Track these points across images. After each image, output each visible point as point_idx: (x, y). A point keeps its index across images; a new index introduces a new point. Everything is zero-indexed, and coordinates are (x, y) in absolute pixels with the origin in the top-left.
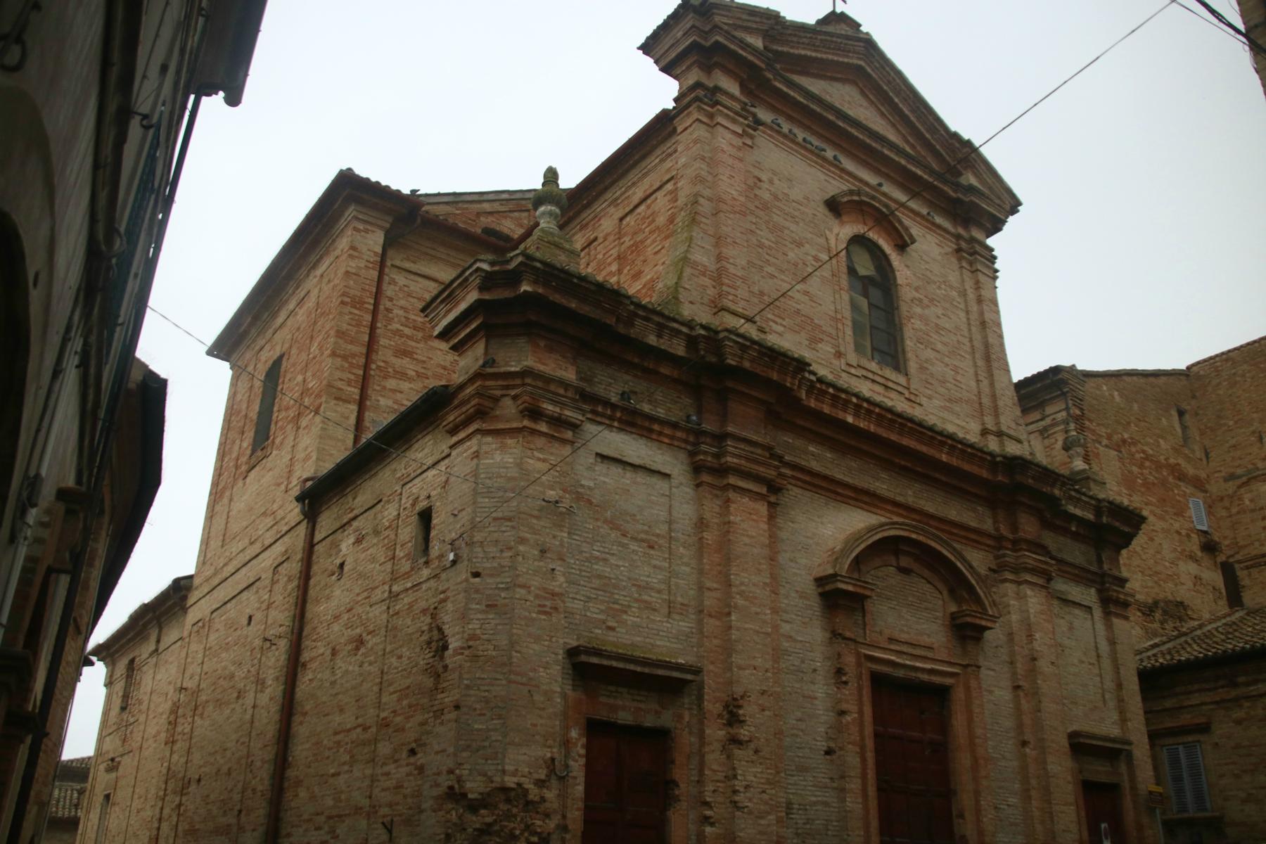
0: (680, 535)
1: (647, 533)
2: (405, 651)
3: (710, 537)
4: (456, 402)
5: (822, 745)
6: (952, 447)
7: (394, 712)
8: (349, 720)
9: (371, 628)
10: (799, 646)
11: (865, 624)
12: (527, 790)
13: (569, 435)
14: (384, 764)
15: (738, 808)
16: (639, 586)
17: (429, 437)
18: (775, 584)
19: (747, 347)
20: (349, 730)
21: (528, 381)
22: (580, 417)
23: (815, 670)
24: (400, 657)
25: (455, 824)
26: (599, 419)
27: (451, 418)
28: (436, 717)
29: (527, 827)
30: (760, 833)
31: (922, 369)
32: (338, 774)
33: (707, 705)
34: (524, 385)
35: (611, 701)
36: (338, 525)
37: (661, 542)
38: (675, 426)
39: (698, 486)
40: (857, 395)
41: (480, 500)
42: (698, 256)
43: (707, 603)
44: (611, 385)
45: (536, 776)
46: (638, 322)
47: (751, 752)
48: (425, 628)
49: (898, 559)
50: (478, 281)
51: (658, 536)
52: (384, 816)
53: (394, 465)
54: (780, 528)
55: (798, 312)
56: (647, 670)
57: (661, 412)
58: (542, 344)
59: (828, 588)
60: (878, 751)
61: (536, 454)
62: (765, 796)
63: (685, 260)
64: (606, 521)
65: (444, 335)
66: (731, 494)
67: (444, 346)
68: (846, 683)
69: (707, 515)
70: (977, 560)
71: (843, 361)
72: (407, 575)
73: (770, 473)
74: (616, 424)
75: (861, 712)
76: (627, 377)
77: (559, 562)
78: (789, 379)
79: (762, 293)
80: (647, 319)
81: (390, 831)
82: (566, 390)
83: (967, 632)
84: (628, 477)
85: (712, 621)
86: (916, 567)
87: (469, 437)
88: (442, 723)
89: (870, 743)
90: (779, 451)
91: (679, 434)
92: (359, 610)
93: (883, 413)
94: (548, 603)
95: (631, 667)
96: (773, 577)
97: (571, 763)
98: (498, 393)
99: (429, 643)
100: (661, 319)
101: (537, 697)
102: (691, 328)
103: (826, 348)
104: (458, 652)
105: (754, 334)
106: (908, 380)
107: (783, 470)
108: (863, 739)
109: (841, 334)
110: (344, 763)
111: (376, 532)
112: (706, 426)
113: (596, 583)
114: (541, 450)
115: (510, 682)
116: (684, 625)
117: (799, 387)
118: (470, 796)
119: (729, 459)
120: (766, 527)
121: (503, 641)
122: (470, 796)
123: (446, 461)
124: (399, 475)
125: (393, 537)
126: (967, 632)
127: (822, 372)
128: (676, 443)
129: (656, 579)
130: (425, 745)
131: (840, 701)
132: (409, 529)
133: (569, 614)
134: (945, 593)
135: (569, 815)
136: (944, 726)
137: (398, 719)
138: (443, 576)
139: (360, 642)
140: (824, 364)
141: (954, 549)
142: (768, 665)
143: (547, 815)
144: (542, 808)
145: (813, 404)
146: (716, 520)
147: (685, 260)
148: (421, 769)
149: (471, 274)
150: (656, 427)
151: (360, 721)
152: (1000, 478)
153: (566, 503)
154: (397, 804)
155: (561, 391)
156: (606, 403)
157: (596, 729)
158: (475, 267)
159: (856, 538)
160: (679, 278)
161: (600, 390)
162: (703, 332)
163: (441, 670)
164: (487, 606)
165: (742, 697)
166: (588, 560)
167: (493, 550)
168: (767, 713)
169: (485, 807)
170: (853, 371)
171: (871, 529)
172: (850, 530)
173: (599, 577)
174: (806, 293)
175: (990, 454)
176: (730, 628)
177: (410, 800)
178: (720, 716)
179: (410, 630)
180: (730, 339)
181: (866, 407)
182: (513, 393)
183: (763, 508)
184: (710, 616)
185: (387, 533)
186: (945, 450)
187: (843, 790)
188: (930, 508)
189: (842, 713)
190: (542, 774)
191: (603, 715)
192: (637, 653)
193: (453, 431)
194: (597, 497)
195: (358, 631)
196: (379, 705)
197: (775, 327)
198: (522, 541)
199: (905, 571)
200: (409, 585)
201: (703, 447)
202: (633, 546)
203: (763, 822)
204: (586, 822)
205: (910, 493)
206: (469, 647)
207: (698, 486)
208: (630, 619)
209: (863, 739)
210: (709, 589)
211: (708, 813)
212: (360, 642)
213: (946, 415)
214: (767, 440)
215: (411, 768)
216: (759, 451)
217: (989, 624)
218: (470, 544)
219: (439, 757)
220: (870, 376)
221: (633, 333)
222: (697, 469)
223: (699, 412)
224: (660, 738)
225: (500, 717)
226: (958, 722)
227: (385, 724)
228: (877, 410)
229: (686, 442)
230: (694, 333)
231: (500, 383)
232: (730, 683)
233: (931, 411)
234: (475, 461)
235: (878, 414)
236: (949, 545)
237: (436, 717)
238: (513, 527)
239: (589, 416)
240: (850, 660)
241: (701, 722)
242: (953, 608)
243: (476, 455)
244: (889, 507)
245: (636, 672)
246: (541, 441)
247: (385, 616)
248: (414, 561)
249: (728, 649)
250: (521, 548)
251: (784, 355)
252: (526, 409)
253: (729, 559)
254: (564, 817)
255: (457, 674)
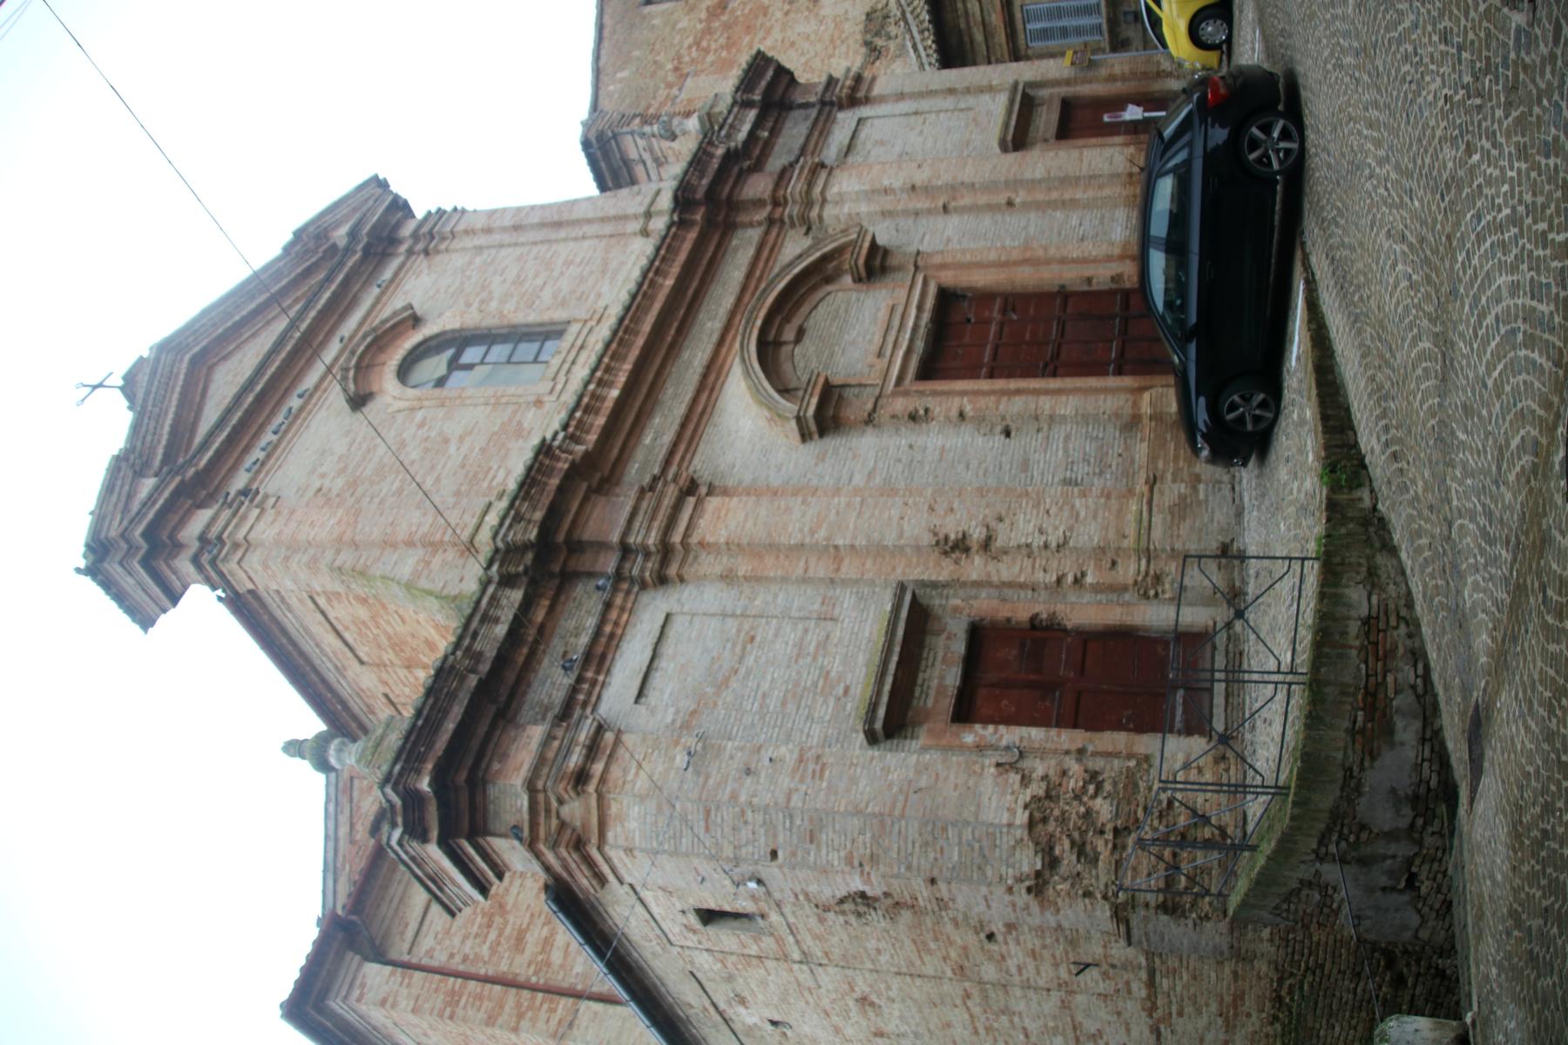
0: (740, 604)
1: (734, 645)
2: (871, 944)
3: (743, 567)
4: (565, 875)
5: (999, 439)
6: (657, 272)
7: (945, 959)
8: (958, 1016)
9: (846, 987)
10: (880, 465)
11: (860, 385)
12: (1033, 797)
13: (609, 736)
14: (1007, 972)
15: (1066, 542)
16: (798, 655)
17: (610, 910)
18: (802, 491)
19: (517, 513)
20: (972, 1016)
21: (540, 785)
22: (589, 721)
23: (911, 447)
24: (879, 951)
25: (1073, 886)
26: (593, 699)
27: (585, 882)
28: (946, 908)
29: (1077, 797)
30: (1095, 517)
31: (564, 303)
32: (1024, 1029)
33: (943, 576)
34: (545, 791)
35: (932, 693)
36: (725, 1027)
37: (746, 627)
38: (608, 605)
39: (682, 580)
40: (587, 384)
41: (683, 849)
42: (405, 572)
43: (822, 574)
44: (551, 683)
45: (1017, 786)
46: (477, 646)
47: (1001, 525)
48: (841, 919)
49: (785, 343)
50: (415, 844)
51: (739, 631)
52: (1070, 972)
53: (647, 955)
54: (740, 482)
55: (483, 450)
56: (897, 649)
57: (591, 622)
58: (496, 766)
59: (813, 427)
60: (1010, 375)
61: (630, 777)
62: (1053, 511)
63: (409, 586)
64: (718, 694)
65: (484, 889)
66: (694, 540)
67: (496, 887)
68: (927, 410)
69: (718, 570)
70: (794, 249)
71: (546, 399)
72: (779, 941)
73: (671, 492)
74: (601, 678)
75: (963, 393)
76: (546, 661)
77: (763, 752)
78: (560, 465)
79: (457, 494)
80: (475, 635)
81: (1087, 966)
82: (555, 738)
83: (876, 264)
84: (666, 664)
85: (844, 569)
86: (796, 322)
87: (607, 860)
88: (953, 900)
89: (999, 384)
90: (647, 480)
91: (618, 601)
92: (825, 1002)
93: (610, 353)
94: (811, 767)
95: (892, 667)
96: (795, 493)
97: (1004, 743)
98: (554, 822)
99: (859, 915)
100: (477, 617)
101: (923, 783)
102: (489, 581)
103: (530, 417)
104: (866, 878)
105: (504, 504)
106: (576, 320)
107: (670, 476)
108: (992, 392)
109: (515, 400)
110: (1011, 1022)
111: (730, 979)
112: (611, 568)
113: (791, 707)
114: (625, 771)
115: (903, 816)
116: (847, 601)
117: (571, 453)
118: (1039, 866)
119: (651, 541)
120: (735, 500)
121: (856, 822)
122: (1039, 866)
123: (638, 889)
124: (658, 949)
125: (734, 958)
126: (876, 264)
127: (556, 425)
128: (629, 605)
129: (791, 634)
130: (981, 922)
131: (948, 418)
132: (723, 937)
133: (826, 742)
134: (829, 288)
135: (1066, 747)
136: (985, 297)
137: (953, 954)
138: (777, 895)
139: (863, 1001)
140: (546, 423)
141: (778, 275)
142: (899, 501)
143: (1064, 773)
144: (1055, 779)
145: (592, 437)
146: (725, 560)
147: (409, 586)
148: (1010, 927)
149: (406, 852)
150: (608, 629)
151: (958, 1002)
152: (698, 217)
153: (690, 741)
154: (1054, 956)
155: (556, 744)
156: (574, 690)
157: (964, 711)
158: (397, 848)
159: (755, 390)
160: (430, 593)
161: (559, 696)
162: (495, 568)
163: (889, 901)
164: (811, 841)
165: (935, 534)
166: (763, 718)
167: (745, 834)
168: (955, 505)
169: (1052, 849)
170: (559, 387)
171: (747, 373)
172: (748, 398)
173: (784, 704)
174: (461, 439)
175: (669, 228)
176: (852, 547)
177: (1048, 941)
178: (956, 562)
179: (846, 938)
180: (505, 535)
181: (601, 374)
182: (554, 804)
183: (713, 503)
184: (838, 570)
185: (729, 965)
186: (660, 280)
187: (1052, 418)
188: (728, 301)
189: (962, 415)
190: (1014, 778)
191: (948, 703)
192: (877, 659)
193: (602, 880)
194: (688, 704)
195: (851, 1003)
196: (938, 978)
197: (499, 479)
198: (734, 797)
199: (800, 334)
200: (791, 939)
201: (635, 572)
202: (750, 661)
203: (1083, 514)
204: (1075, 726)
205: (709, 325)
206: (861, 865)
207: (682, 580)
208: (836, 668)
209: (992, 392)
210: (806, 571)
211: (1070, 579)
212: (863, 1001)
213: (621, 278)
214: (633, 494)
215: (1009, 938)
216: (644, 504)
217: (869, 238)
218: (737, 861)
219: (993, 905)
220: (566, 366)
221: (490, 653)
222: (662, 580)
223: (591, 575)
224: (979, 635)
225: (944, 829)
226: (981, 279)
227: (960, 970)
228: (606, 360)
229: (628, 593)
230: (496, 578)
231: (542, 819)
232: (918, 548)
233: (614, 295)
234: (636, 853)
235: (612, 358)
236: (772, 282)
237: (946, 908)
238: (718, 808)
239: (589, 710)
240: (900, 405)
241: (964, 585)
242: (847, 280)
243: (629, 851)
244: (724, 350)
245: (899, 663)
246: (616, 772)
247: (831, 970)
248: (761, 932)
249: (878, 551)
250: (743, 798)
251: (529, 469)
252: (575, 788)
253: (770, 545)
254: (1067, 752)
255: (893, 881)
